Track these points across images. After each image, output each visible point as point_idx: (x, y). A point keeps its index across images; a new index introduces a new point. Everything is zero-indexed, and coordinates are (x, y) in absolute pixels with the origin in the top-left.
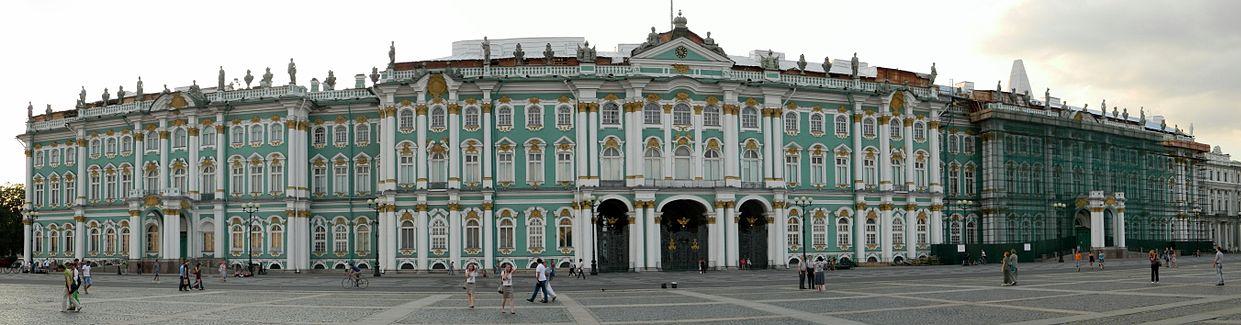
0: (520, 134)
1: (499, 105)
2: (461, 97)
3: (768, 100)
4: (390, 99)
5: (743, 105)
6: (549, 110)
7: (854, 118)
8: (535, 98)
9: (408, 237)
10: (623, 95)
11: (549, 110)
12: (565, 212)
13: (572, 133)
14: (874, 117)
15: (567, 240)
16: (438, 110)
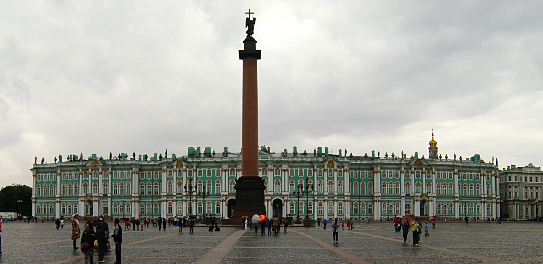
0: (204, 178)
1: (198, 169)
2: (187, 167)
3: (283, 166)
4: (165, 167)
5: (275, 168)
6: (214, 171)
7: (314, 171)
8: (209, 167)
9: (170, 210)
10: (236, 166)
11: (214, 171)
12: (218, 202)
13: (221, 178)
14: (322, 169)
15: (218, 211)
16: (180, 171)
